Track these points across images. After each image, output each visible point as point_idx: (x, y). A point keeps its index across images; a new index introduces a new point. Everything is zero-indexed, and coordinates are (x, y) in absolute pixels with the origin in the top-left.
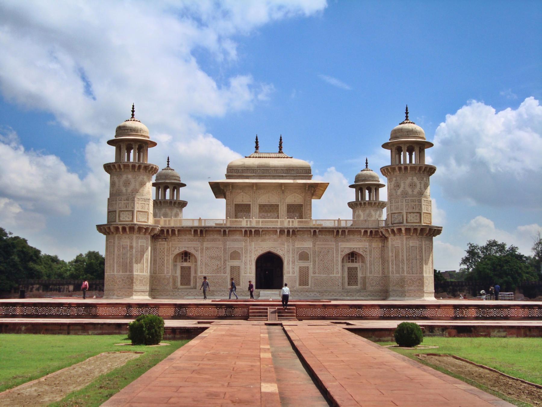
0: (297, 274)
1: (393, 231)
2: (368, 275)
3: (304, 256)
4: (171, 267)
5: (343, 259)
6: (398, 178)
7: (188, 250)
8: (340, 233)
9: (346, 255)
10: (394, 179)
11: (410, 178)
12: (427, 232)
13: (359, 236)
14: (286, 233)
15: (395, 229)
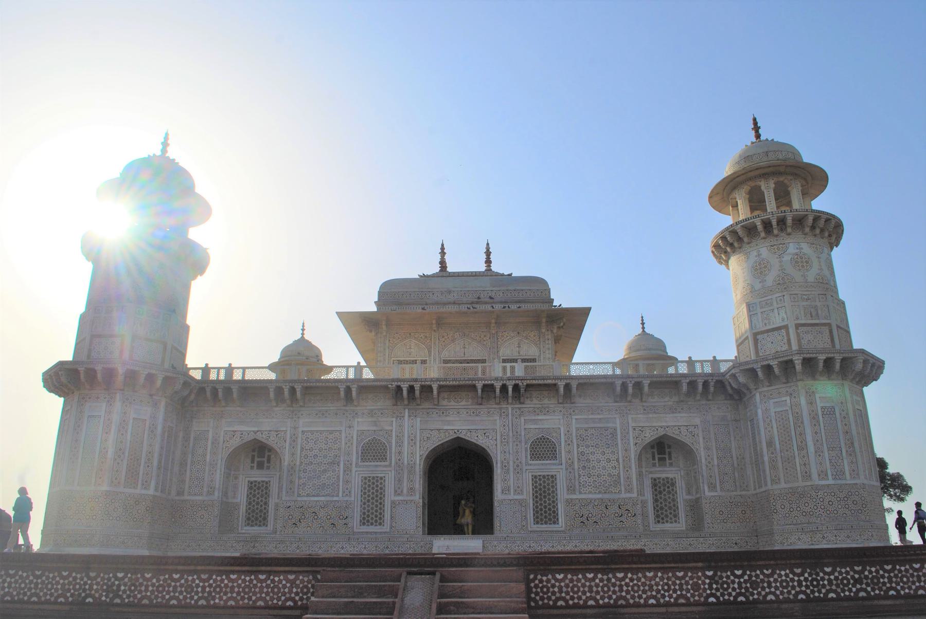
0: (527, 495)
1: (768, 369)
2: (708, 493)
3: (543, 448)
4: (218, 477)
5: (640, 459)
6: (765, 252)
7: (262, 437)
8: (630, 390)
9: (645, 448)
10: (755, 253)
11: (792, 249)
12: (859, 366)
13: (676, 399)
14: (498, 391)
15: (774, 363)
